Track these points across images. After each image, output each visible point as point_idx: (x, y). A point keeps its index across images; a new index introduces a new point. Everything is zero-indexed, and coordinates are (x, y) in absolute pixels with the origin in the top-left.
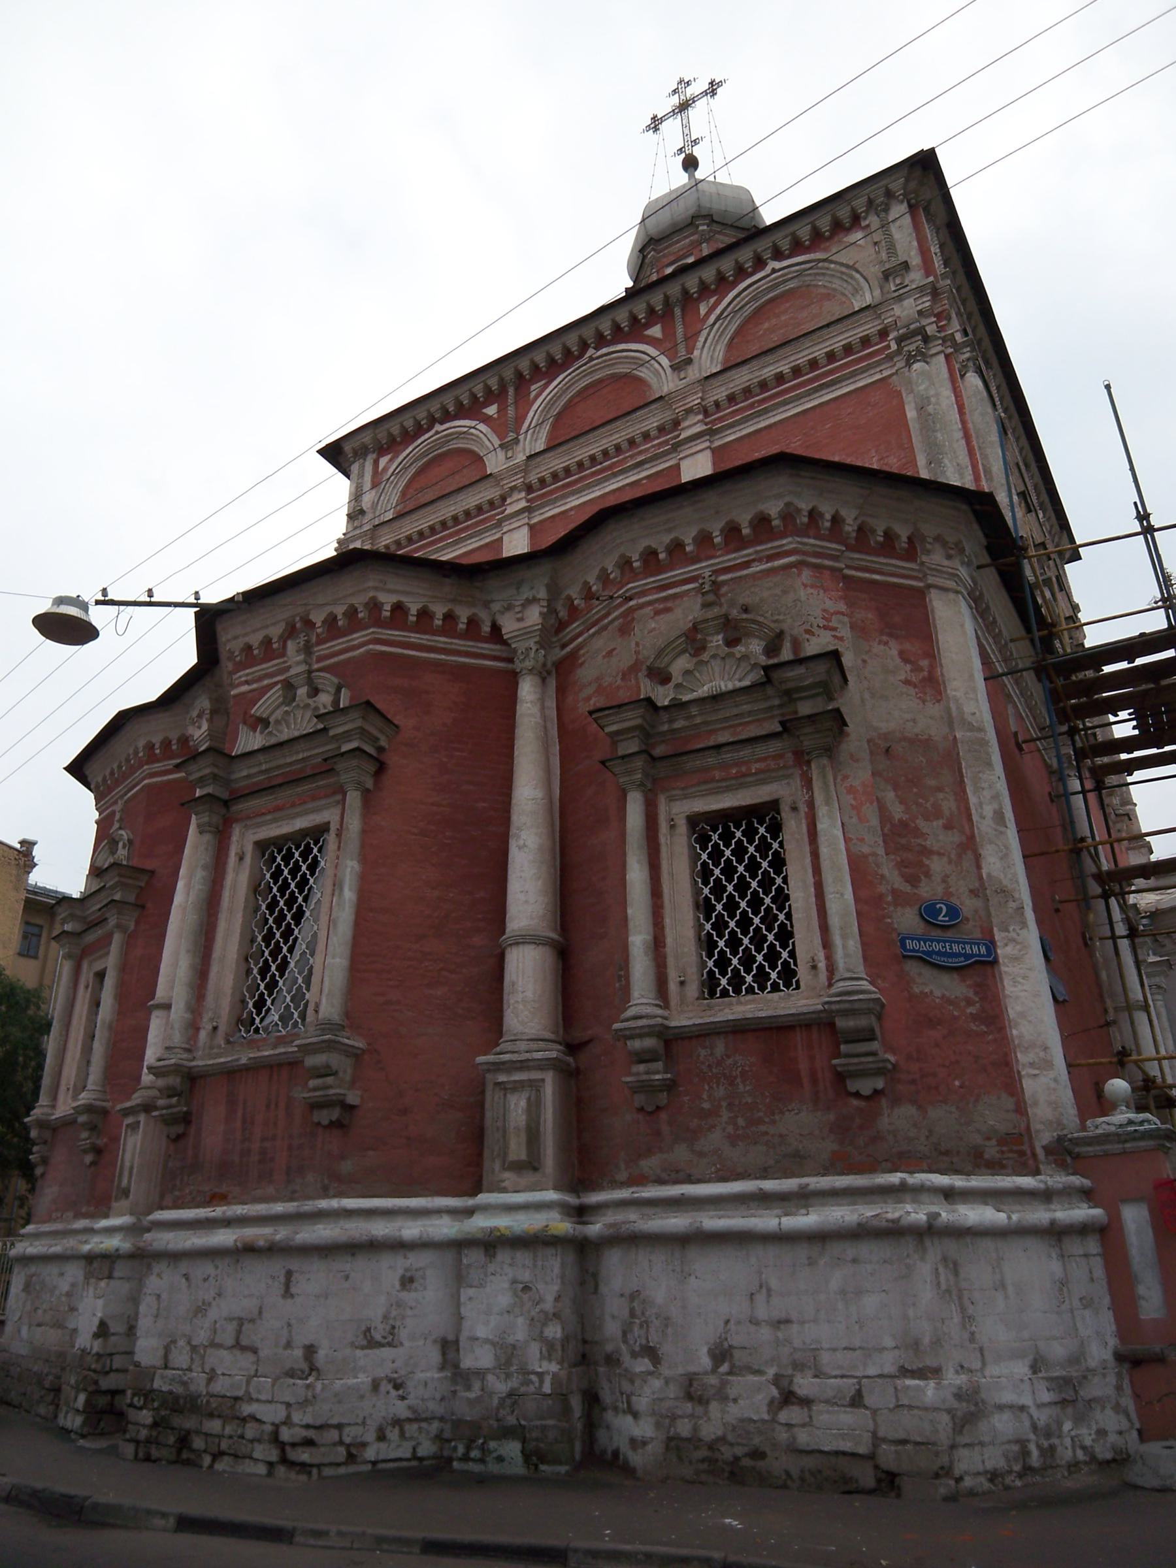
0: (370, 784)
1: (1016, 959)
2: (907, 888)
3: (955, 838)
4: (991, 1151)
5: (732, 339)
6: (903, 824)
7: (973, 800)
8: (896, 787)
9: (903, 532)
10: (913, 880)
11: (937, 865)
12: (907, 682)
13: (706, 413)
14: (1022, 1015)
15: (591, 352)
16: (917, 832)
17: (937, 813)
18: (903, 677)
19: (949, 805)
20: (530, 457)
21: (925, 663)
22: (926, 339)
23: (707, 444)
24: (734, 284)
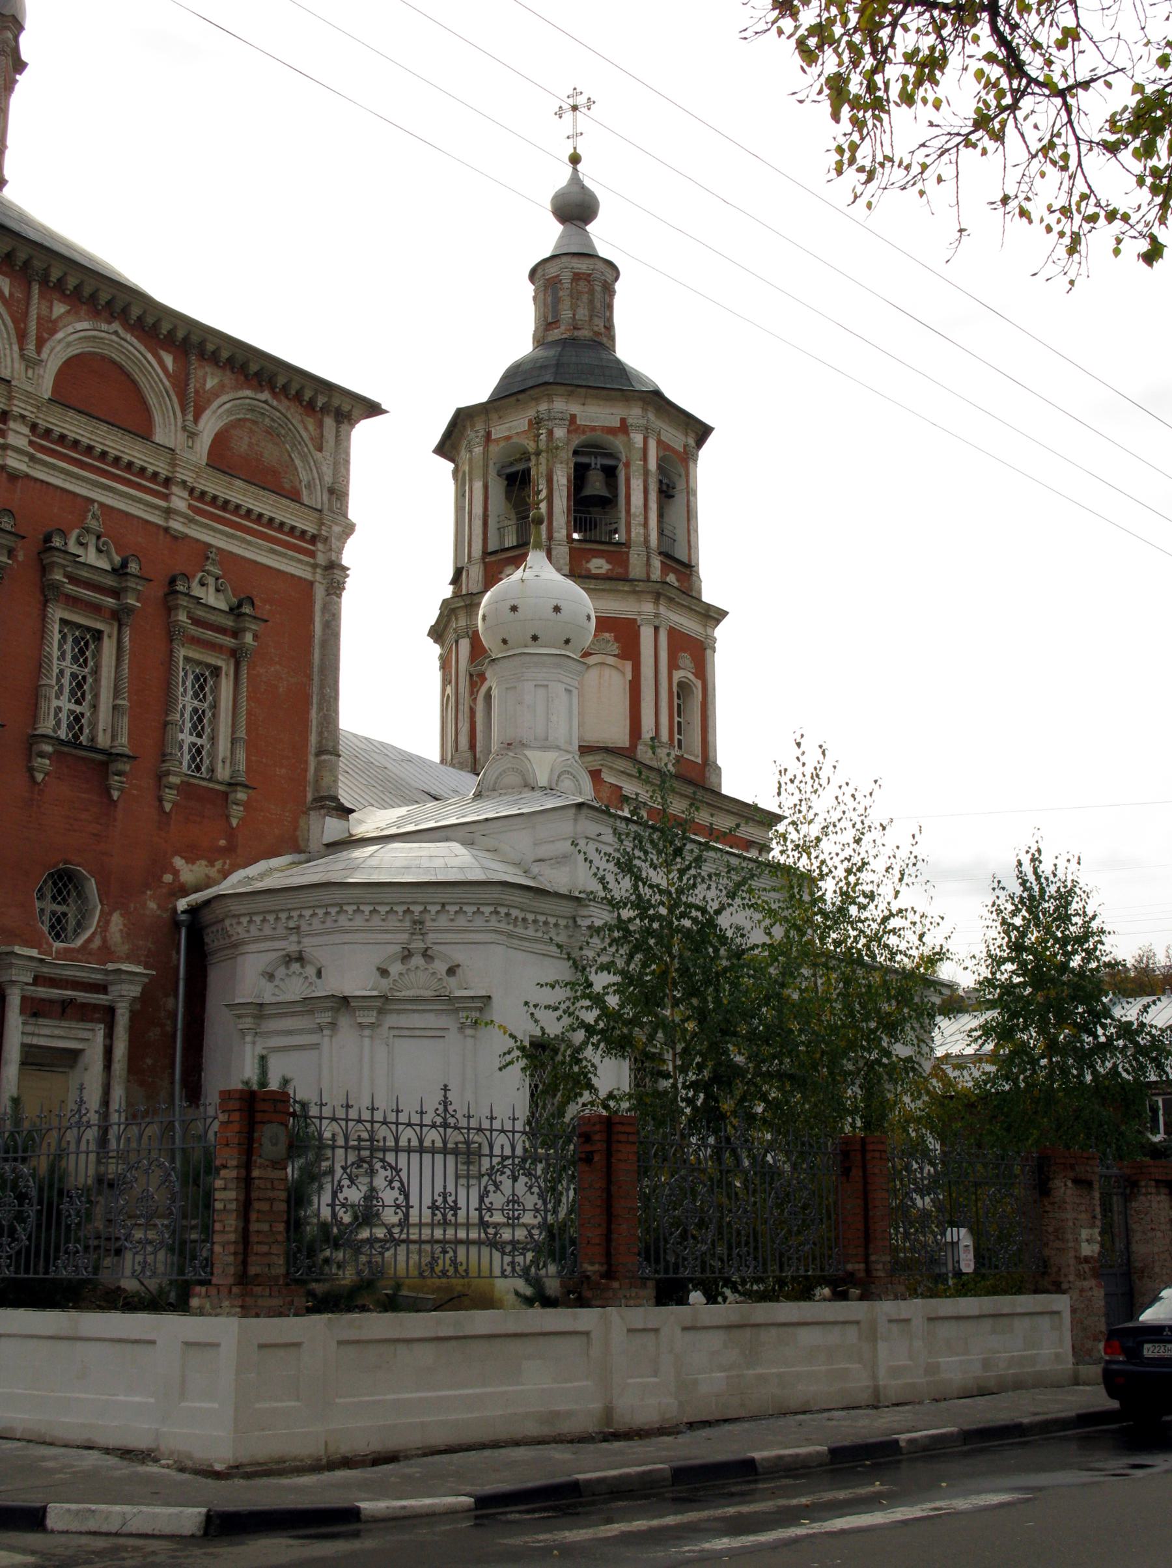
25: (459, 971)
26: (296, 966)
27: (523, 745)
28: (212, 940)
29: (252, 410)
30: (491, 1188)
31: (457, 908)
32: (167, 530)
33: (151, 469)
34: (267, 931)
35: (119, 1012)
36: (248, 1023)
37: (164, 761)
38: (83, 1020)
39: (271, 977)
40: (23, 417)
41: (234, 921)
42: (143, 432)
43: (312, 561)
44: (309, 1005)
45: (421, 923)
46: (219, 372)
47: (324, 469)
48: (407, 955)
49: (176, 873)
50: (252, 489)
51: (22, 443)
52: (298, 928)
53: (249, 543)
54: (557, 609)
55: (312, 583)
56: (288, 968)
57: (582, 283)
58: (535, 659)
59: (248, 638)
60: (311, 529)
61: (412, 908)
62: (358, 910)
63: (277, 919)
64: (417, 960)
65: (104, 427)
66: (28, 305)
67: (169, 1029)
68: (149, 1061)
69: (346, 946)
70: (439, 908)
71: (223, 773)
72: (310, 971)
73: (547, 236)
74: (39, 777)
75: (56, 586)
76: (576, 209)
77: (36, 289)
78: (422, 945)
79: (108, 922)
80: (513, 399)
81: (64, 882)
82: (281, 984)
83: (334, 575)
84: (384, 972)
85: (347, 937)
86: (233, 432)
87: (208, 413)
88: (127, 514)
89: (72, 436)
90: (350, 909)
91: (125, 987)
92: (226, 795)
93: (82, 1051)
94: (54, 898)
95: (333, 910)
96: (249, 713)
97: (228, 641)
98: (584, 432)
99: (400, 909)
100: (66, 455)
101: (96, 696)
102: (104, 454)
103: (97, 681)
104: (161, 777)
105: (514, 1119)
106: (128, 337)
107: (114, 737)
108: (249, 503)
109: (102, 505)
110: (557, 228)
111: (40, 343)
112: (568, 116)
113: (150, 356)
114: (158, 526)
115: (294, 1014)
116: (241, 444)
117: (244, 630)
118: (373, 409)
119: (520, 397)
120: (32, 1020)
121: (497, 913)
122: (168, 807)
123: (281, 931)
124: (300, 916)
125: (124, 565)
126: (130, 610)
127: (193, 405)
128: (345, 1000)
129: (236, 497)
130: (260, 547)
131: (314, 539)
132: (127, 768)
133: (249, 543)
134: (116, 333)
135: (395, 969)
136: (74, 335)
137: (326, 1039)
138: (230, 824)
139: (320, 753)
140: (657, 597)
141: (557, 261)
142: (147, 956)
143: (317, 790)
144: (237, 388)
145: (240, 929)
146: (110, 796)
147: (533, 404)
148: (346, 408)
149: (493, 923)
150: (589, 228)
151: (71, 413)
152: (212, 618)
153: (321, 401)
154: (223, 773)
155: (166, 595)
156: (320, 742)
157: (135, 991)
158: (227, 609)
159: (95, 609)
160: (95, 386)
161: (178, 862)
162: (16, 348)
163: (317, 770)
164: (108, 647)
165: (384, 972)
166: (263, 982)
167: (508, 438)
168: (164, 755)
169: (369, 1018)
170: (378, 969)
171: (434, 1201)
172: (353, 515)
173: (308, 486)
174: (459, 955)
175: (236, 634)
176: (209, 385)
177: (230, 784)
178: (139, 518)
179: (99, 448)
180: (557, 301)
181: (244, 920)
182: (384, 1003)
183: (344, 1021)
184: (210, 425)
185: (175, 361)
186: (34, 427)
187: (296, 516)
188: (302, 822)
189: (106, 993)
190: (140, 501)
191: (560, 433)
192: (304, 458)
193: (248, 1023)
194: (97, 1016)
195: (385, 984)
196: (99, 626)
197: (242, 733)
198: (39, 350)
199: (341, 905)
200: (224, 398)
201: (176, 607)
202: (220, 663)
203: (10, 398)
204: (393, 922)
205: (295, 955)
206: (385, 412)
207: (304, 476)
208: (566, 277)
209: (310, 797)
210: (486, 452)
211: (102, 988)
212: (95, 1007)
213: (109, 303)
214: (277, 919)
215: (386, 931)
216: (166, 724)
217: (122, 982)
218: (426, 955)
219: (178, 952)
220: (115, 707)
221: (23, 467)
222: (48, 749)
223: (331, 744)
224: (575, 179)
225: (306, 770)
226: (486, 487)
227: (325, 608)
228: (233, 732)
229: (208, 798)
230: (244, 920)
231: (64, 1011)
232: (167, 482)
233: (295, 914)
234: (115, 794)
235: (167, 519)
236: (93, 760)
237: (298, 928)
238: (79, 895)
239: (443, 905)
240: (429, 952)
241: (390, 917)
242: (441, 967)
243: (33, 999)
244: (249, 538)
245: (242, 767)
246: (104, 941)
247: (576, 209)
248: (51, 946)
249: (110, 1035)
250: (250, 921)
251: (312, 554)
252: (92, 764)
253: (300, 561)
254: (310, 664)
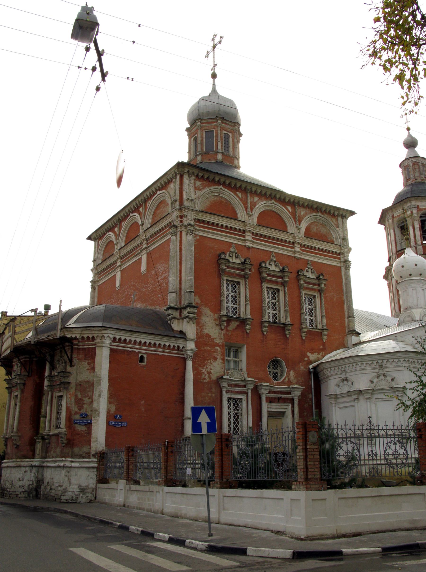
0: (22, 387)
1: (95, 423)
2: (78, 411)
3: (90, 400)
4: (84, 455)
5: (153, 215)
6: (80, 399)
7: (94, 393)
8: (81, 392)
9: (91, 336)
10: (80, 410)
11: (85, 406)
12: (88, 369)
13: (147, 241)
14: (94, 432)
15: (131, 215)
16: (83, 400)
17: (88, 396)
18: (87, 368)
19: (90, 394)
20: (119, 249)
21: (92, 364)
22: (176, 227)
23: (145, 252)
24: (154, 195)
25: (395, 380)
26: (345, 382)
27: (411, 308)
28: (321, 376)
30: (388, 448)
31: (392, 360)
32: (295, 257)
33: (288, 240)
34: (336, 372)
35: (295, 400)
36: (333, 400)
37: (301, 325)
38: (284, 403)
39: (338, 386)
40: (249, 231)
41: (326, 370)
42: (284, 230)
43: (340, 260)
44: (350, 394)
45: (382, 366)
46: (305, 209)
47: (340, 233)
48: (378, 376)
49: (308, 357)
50: (319, 242)
51: (250, 238)
52: (345, 370)
53: (320, 258)
54: (416, 265)
55: (340, 267)
56: (343, 383)
57: (416, 166)
58: (411, 281)
59: (323, 286)
60: (338, 251)
61: (378, 361)
62: (362, 364)
63: (338, 368)
64: (382, 377)
65: (273, 230)
66: (247, 199)
67: (310, 404)
68: (305, 414)
69: (360, 375)
70: (387, 361)
71: (320, 326)
72: (350, 383)
73: (403, 153)
74: (265, 333)
75: (264, 278)
76: (411, 144)
77: (249, 194)
78: (383, 372)
79: (289, 374)
80: (399, 204)
81: (276, 363)
82: (342, 388)
83: (347, 264)
84: (372, 382)
85: (360, 372)
86: (312, 226)
87: (303, 222)
88: (283, 254)
89: (264, 234)
90: (360, 363)
91: (296, 392)
92: (321, 333)
93: (285, 412)
94: (273, 368)
95: (355, 364)
96: (325, 308)
97: (317, 287)
98: (422, 210)
99: (375, 362)
100: (263, 240)
101: (279, 308)
102: (274, 238)
103: (279, 304)
104: (301, 329)
105: (394, 426)
106: (277, 204)
107: (286, 320)
108: (318, 246)
109: (275, 253)
110: (406, 150)
111: (252, 209)
112: (404, 117)
113: (284, 208)
114: (292, 257)
115: (346, 397)
116: (314, 229)
117: (321, 283)
118: (352, 213)
119: (401, 203)
120: (270, 404)
121: (405, 360)
122: (304, 338)
123: (340, 372)
124: (345, 367)
125: (283, 269)
126: (286, 282)
127: (298, 220)
128: (361, 391)
129: (314, 245)
130: (322, 258)
131: (339, 254)
132: (290, 328)
133: (320, 258)
134: (273, 203)
135: (375, 380)
136: (261, 205)
137: (356, 404)
138: (323, 342)
139: (348, 318)
141: (407, 160)
142: (302, 383)
143: (349, 329)
144: (310, 213)
145: (328, 372)
146: (286, 337)
147: (405, 204)
148: (344, 214)
149: (404, 364)
150: (416, 149)
151: (263, 228)
152: (311, 281)
153: (336, 213)
154: (320, 326)
155: (297, 276)
156: (348, 314)
157: (299, 393)
158: (315, 278)
159: (276, 283)
160: (269, 219)
161: (309, 354)
162: (245, 212)
163: (348, 323)
164: (281, 293)
165: (372, 382)
166: (336, 388)
167: (399, 216)
168: (301, 323)
169: (369, 396)
170: (370, 381)
171: (369, 453)
172: (350, 245)
173: (336, 239)
174: (395, 375)
175: (319, 285)
176: (302, 214)
177: (322, 330)
178: (286, 255)
179: (272, 236)
180: (409, 172)
181: (329, 369)
182: (373, 391)
183: (361, 397)
184: (304, 225)
185: (291, 208)
186: (253, 233)
187: (333, 248)
188: (345, 339)
189: (291, 394)
190: (286, 250)
191: (415, 212)
192: (333, 231)
193: (333, 400)
194: (288, 401)
195: (372, 385)
197: (324, 314)
198: (252, 211)
199: (356, 362)
200: (307, 217)
201: (300, 279)
202: (315, 294)
203: (245, 226)
204: (373, 366)
205: (345, 379)
206: (356, 213)
207: (334, 236)
208: (411, 165)
209: (347, 331)
210: (393, 221)
211: (290, 393)
212: (288, 399)
213: (270, 195)
214: (338, 368)
215: (372, 369)
216: (301, 314)
217: (295, 391)
218: (384, 375)
219: (311, 381)
220: (285, 311)
221: (251, 245)
222: (267, 325)
223: (351, 314)
224: (409, 135)
225: (345, 323)
226: (394, 231)
227: (345, 274)
228: (321, 314)
229: (316, 335)
230: (329, 369)
231: (279, 401)
232: (293, 243)
233: (343, 366)
234: (288, 336)
235: (294, 254)
236: (280, 327)
237: (345, 370)
238: (280, 366)
239: (388, 360)
240: (385, 375)
241: (372, 364)
242: (389, 379)
243: (269, 398)
244: (320, 256)
245: (325, 324)
246: (289, 379)
247: (411, 144)
248: (273, 382)
249: (293, 406)
250: (331, 370)
251: (339, 258)
252: (280, 328)
253: (336, 261)
254: (342, 291)
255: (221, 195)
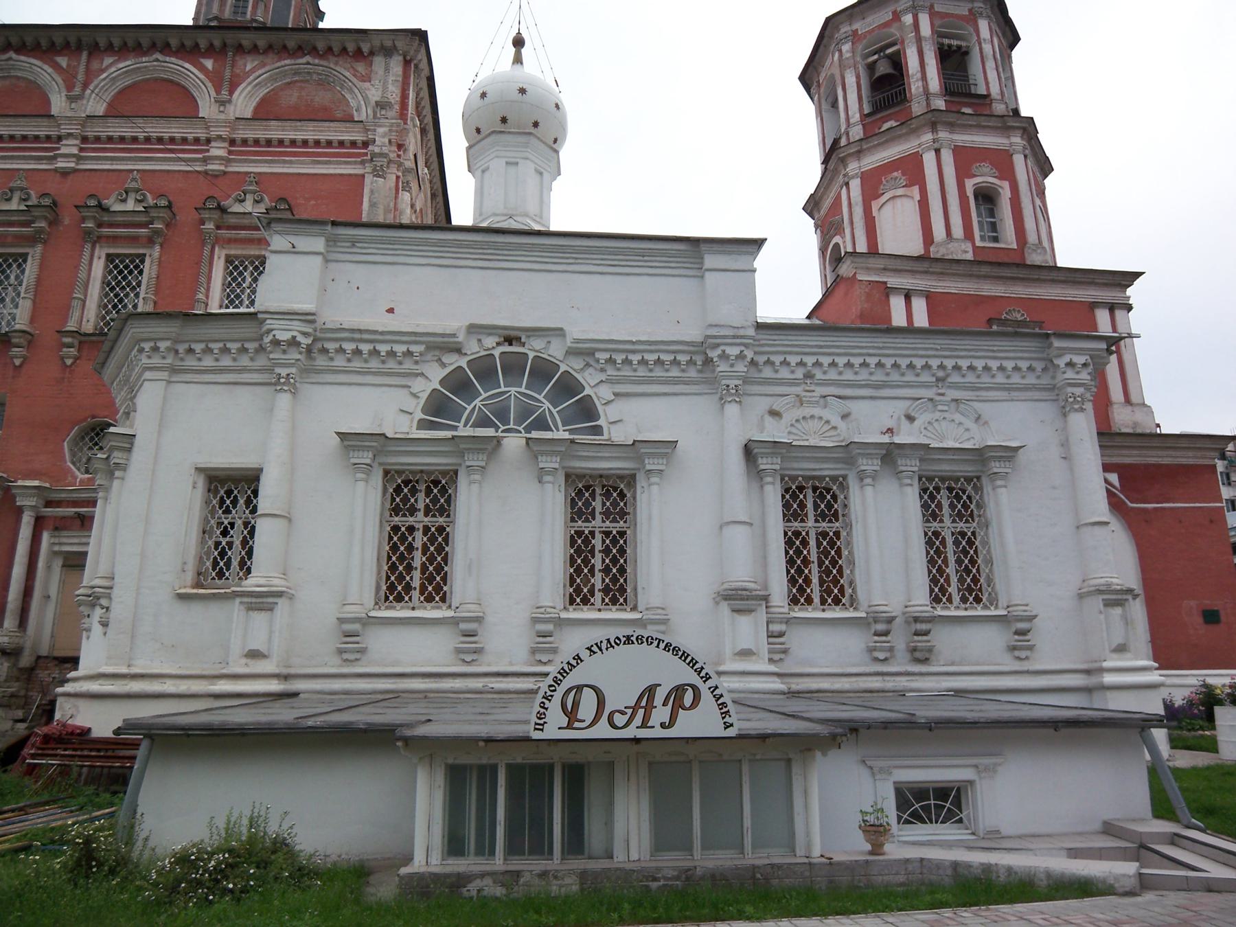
29: (295, 74)
32: (206, 173)
33: (190, 137)
74: (69, 362)
106: (168, 59)
108: (289, 135)
116: (291, 98)
129: (275, 135)
131: (365, 144)
134: (157, 60)
136: (116, 71)
140: (934, 127)
148: (388, 43)
153: (366, 49)
159: (134, 240)
178: (179, 171)
196: (141, 251)
207: (353, 103)
243: (55, 517)
248: (76, 478)
255: (13, 73)
